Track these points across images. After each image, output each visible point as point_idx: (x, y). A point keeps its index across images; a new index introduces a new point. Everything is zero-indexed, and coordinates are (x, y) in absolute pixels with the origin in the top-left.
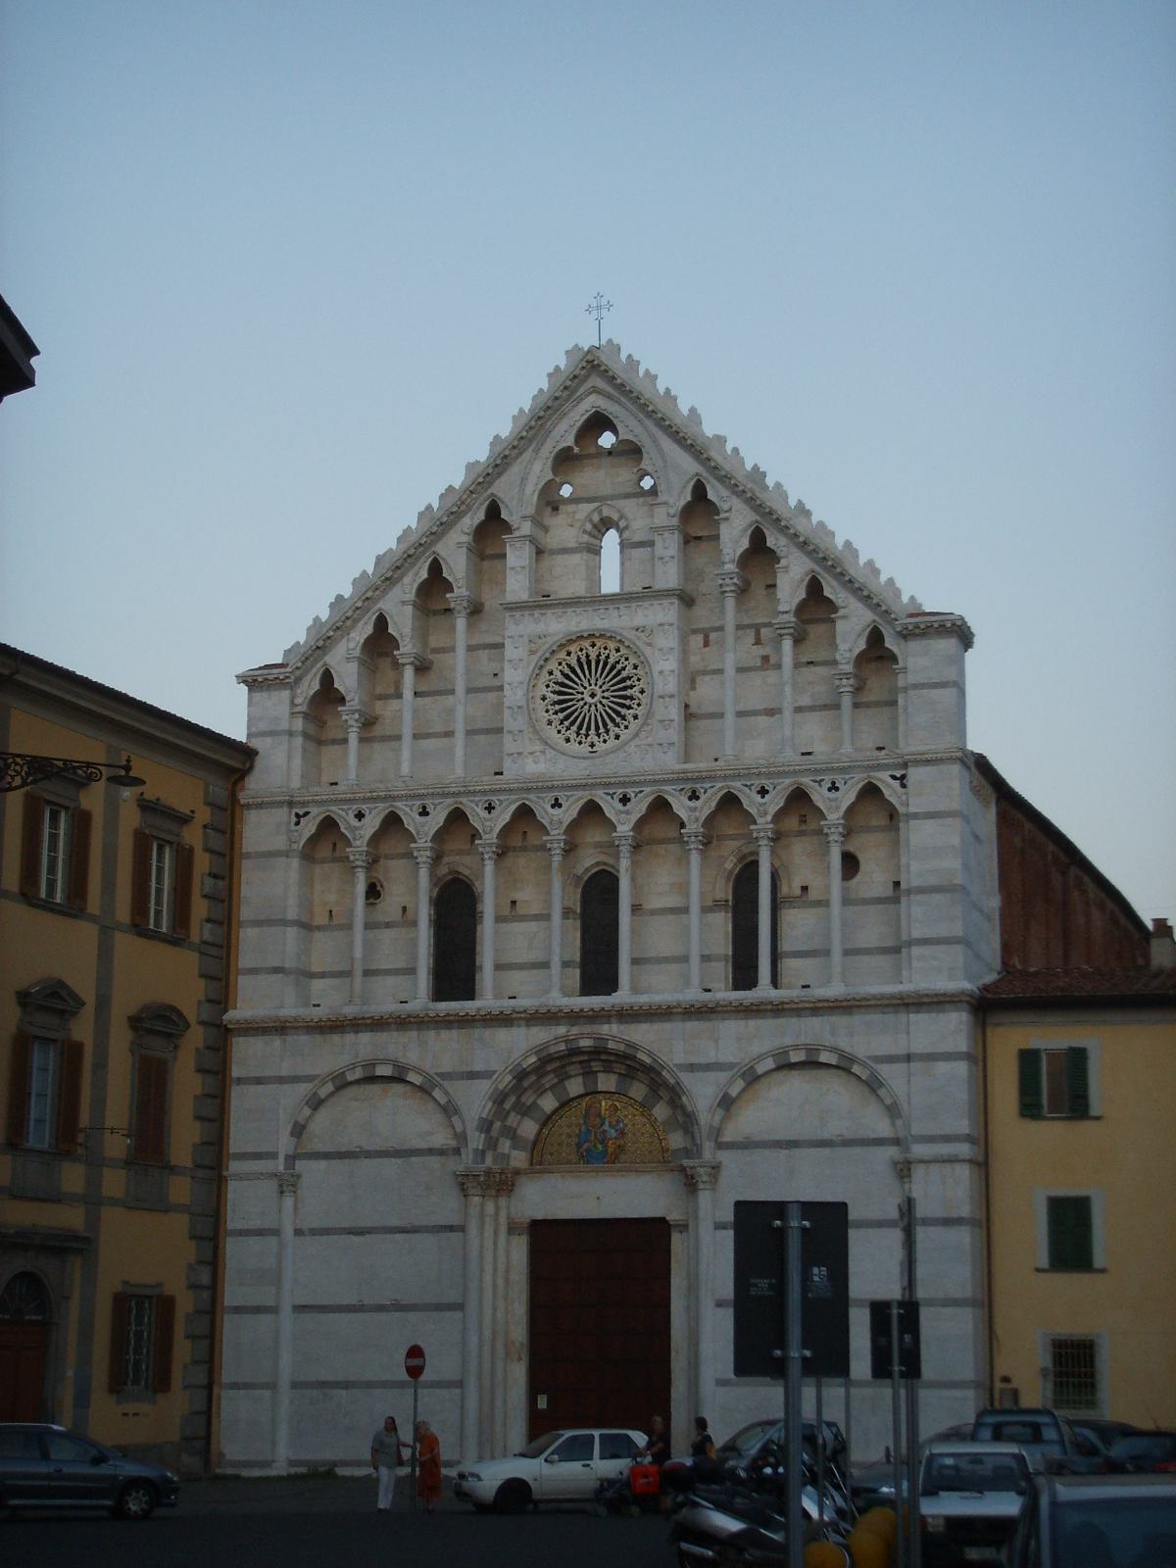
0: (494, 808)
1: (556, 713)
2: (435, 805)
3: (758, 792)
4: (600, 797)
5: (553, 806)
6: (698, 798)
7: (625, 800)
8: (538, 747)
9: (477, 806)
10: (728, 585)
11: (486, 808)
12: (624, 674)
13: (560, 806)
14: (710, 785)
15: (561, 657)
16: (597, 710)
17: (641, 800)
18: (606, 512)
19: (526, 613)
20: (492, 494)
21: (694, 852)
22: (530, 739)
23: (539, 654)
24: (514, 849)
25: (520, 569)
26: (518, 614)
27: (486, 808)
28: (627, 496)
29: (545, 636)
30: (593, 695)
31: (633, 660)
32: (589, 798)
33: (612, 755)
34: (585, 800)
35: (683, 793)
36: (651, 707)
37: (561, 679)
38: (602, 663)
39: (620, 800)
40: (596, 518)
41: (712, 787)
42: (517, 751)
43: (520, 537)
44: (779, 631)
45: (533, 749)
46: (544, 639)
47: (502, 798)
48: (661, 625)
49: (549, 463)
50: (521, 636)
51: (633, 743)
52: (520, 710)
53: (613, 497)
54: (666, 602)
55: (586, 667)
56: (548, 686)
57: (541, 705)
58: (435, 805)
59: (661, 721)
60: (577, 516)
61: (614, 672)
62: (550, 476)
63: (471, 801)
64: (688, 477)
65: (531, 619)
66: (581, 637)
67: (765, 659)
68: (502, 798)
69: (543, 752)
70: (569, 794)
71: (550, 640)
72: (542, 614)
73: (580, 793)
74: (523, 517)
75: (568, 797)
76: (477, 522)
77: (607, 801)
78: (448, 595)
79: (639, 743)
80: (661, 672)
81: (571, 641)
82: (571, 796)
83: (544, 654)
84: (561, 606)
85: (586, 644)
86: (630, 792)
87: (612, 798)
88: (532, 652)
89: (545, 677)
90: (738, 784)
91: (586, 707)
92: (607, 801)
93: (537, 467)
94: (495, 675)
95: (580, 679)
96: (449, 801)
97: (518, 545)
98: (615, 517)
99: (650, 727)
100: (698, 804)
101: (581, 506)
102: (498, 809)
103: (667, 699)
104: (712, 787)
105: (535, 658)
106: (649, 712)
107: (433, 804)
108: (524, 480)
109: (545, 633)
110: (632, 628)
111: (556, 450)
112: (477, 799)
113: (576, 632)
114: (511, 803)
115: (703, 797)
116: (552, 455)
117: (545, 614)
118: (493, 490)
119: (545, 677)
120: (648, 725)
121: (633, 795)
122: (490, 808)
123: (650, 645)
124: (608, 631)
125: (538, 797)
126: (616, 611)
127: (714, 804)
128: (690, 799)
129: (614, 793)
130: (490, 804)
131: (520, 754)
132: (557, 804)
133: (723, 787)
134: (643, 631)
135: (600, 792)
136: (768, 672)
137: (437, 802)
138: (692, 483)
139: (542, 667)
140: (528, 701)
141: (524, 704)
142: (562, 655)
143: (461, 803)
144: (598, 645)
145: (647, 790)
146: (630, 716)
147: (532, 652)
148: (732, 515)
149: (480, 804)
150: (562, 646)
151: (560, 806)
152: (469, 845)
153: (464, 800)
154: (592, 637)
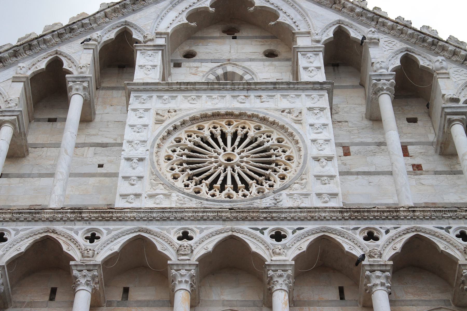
0: (98, 238)
1: (183, 171)
2: (17, 232)
3: (457, 236)
4: (244, 230)
5: (179, 239)
6: (377, 239)
7: (278, 236)
8: (160, 189)
9: (77, 233)
10: (384, 84)
11: (86, 238)
12: (266, 145)
13: (191, 238)
14: (392, 226)
15: (192, 129)
16: (234, 170)
17: (299, 239)
18: (230, 69)
19: (155, 95)
20: (126, 23)
21: (379, 287)
22: (151, 184)
23: (165, 124)
24: (110, 304)
25: (150, 67)
26: (144, 95)
27: (86, 238)
28: (251, 60)
29: (175, 111)
30: (229, 160)
31: (275, 136)
32: (230, 233)
33: (258, 201)
34: (226, 235)
35: (358, 231)
36: (303, 167)
37: (191, 145)
38: (239, 139)
39: (272, 237)
40: (220, 72)
41: (395, 228)
42: (134, 193)
43: (154, 46)
44: (448, 117)
45: (158, 191)
46: (174, 113)
47: (111, 227)
48: (310, 109)
49: (184, 15)
50: (147, 110)
51: (284, 192)
52: (141, 163)
53: (239, 60)
54: (315, 94)
55: (220, 140)
56: (174, 151)
57: (165, 166)
58: (17, 232)
59: (318, 177)
60: (200, 69)
61: (254, 145)
62: (186, 21)
63: (71, 229)
64: (328, 23)
65: (160, 101)
66: (216, 115)
67: (418, 167)
68: (111, 227)
69: (167, 196)
70: (203, 227)
71: (185, 113)
72: (173, 97)
73: (217, 226)
74: (157, 34)
75: (202, 231)
76: (105, 39)
77: (255, 237)
78: (67, 76)
79: (291, 192)
80: (314, 141)
81: (205, 117)
82: (206, 229)
83: (175, 121)
84: (195, 92)
85: (223, 123)
86: (287, 227)
87: (263, 233)
88: (159, 122)
89: (171, 140)
90: (429, 226)
91: (222, 168)
92: (255, 237)
93: (172, 15)
94: (101, 166)
95: (212, 147)
96: (39, 227)
97: (150, 52)
98: (240, 72)
99: (304, 181)
100: (377, 242)
101: (203, 64)
102: (104, 238)
103: (322, 160)
104: (395, 228)
105: (160, 127)
106: (303, 167)
107: (14, 230)
108: (160, 17)
109: (176, 109)
110: (277, 110)
111: (191, 8)
112: (76, 227)
113: (212, 109)
114: (124, 234)
115: (384, 238)
116: (188, 10)
117: (177, 96)
118: (131, 19)
119: (171, 140)
120: (302, 180)
121: (290, 231)
122: (92, 238)
123: (299, 122)
124: (250, 110)
125: (162, 229)
126: (258, 100)
127: (399, 246)
128: (366, 239)
129: (265, 229)
130: (93, 235)
131: (137, 196)
132: (185, 236)
133: (407, 229)
134: (289, 113)
135: (246, 226)
136: (421, 176)
137: (20, 228)
138: (334, 28)
139: (169, 133)
140: (152, 154)
141: (147, 157)
142: (194, 128)
143: (54, 232)
144: (235, 123)
145: (309, 226)
146: (276, 176)
147: (159, 122)
148: (381, 42)
149: (80, 232)
150: (194, 120)
151: (191, 238)
152: (47, 298)
153: (59, 227)
154: (229, 116)
